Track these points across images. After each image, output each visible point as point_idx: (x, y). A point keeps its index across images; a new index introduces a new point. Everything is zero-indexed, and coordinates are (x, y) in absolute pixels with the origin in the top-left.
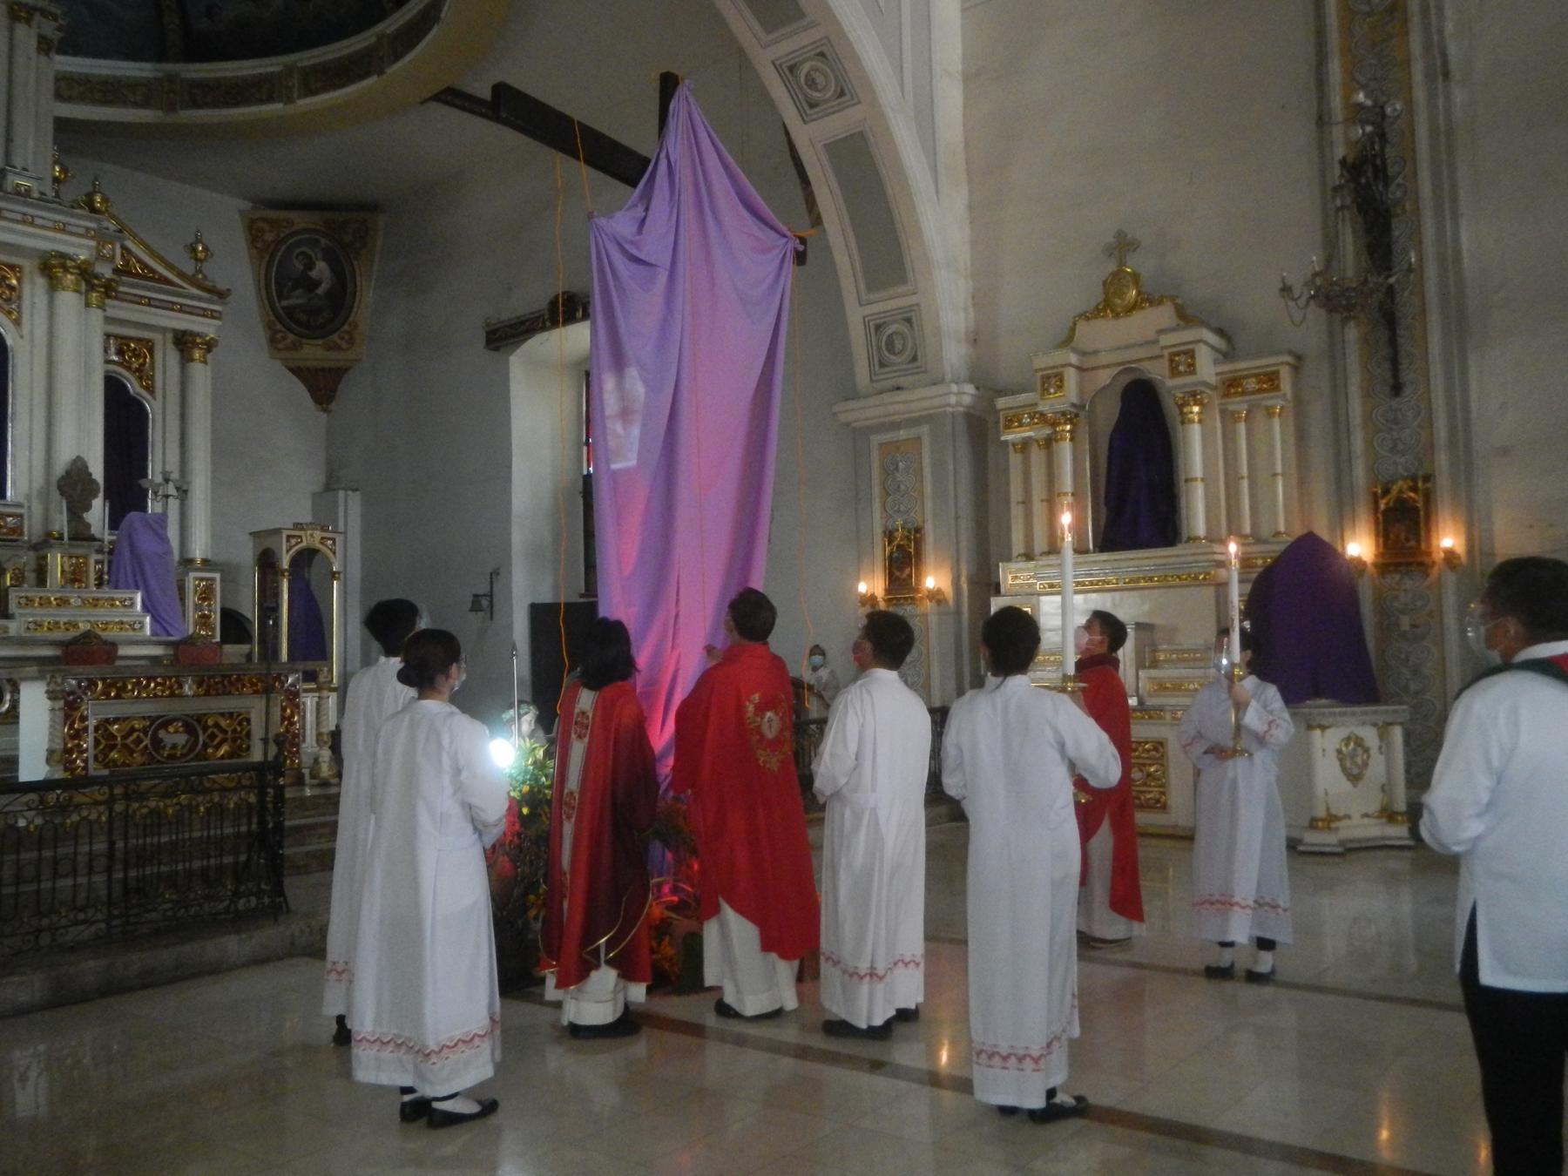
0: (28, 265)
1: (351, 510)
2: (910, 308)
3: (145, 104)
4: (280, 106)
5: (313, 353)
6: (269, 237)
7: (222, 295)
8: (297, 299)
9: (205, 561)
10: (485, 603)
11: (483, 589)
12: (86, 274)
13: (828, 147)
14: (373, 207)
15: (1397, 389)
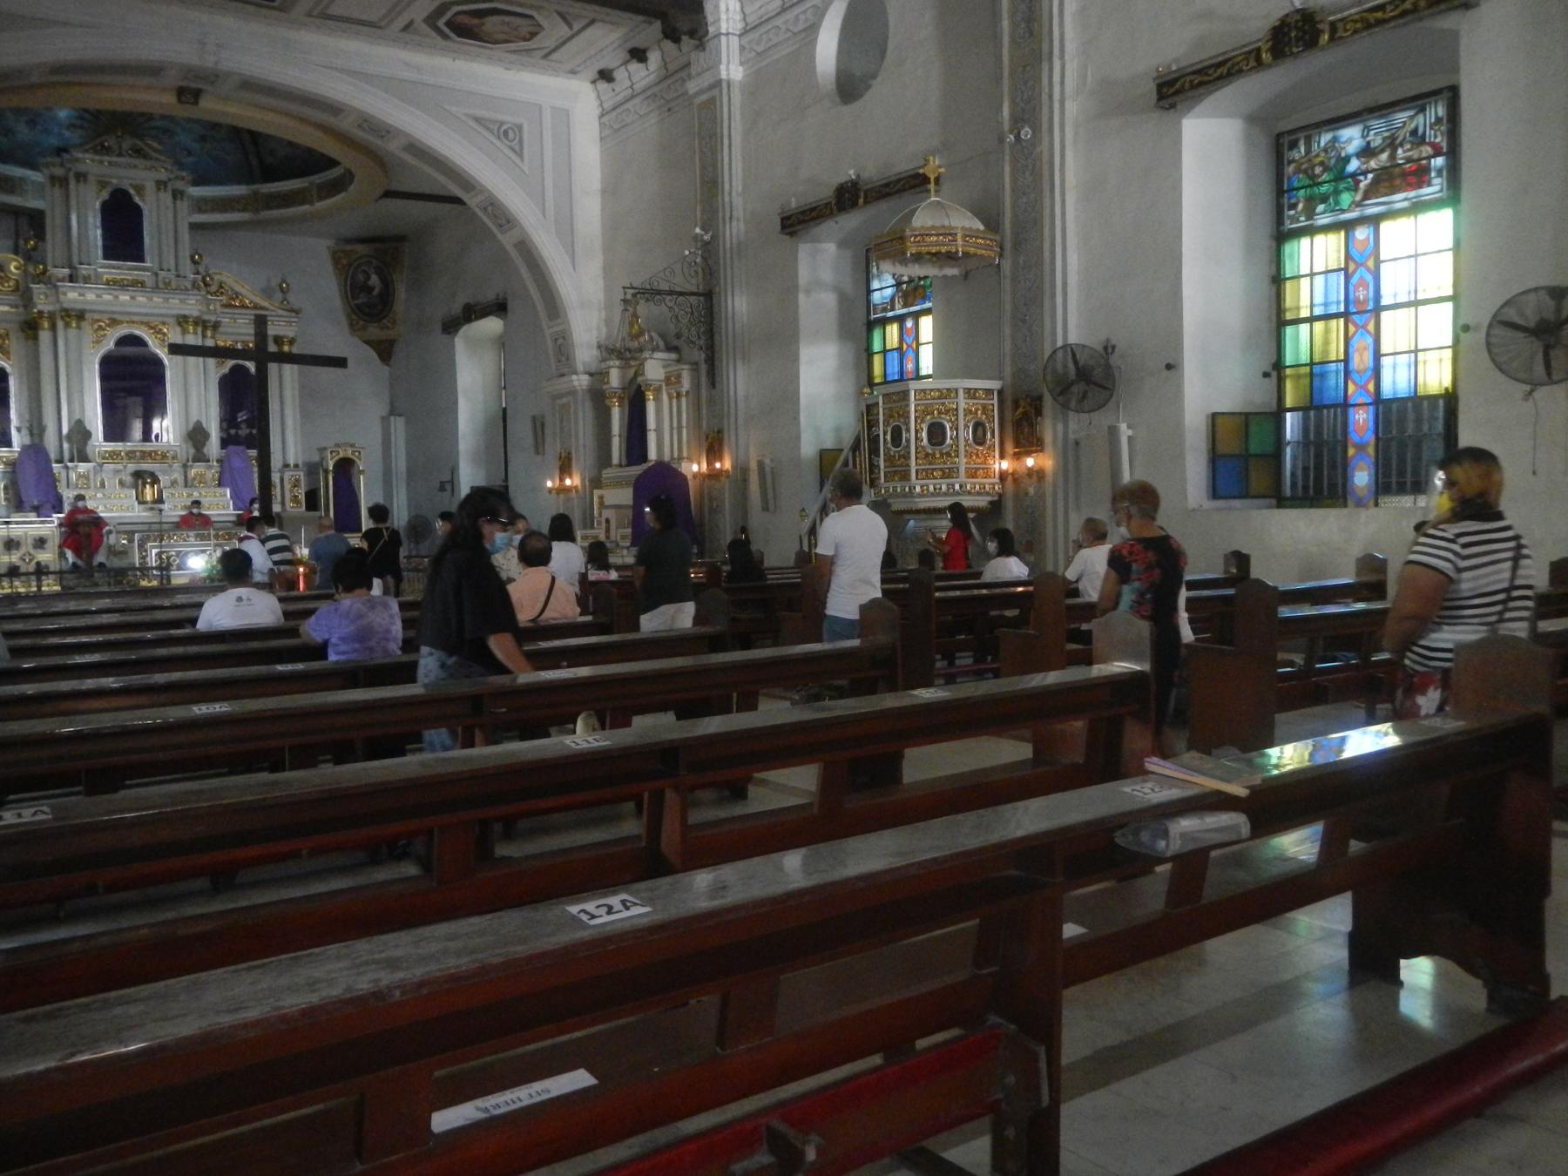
0: (172, 320)
1: (399, 425)
2: (564, 331)
3: (244, 210)
4: (306, 207)
5: (374, 331)
6: (345, 262)
7: (297, 312)
8: (362, 299)
9: (296, 466)
10: (448, 487)
11: (448, 478)
12: (196, 323)
13: (515, 246)
14: (401, 239)
15: (713, 384)
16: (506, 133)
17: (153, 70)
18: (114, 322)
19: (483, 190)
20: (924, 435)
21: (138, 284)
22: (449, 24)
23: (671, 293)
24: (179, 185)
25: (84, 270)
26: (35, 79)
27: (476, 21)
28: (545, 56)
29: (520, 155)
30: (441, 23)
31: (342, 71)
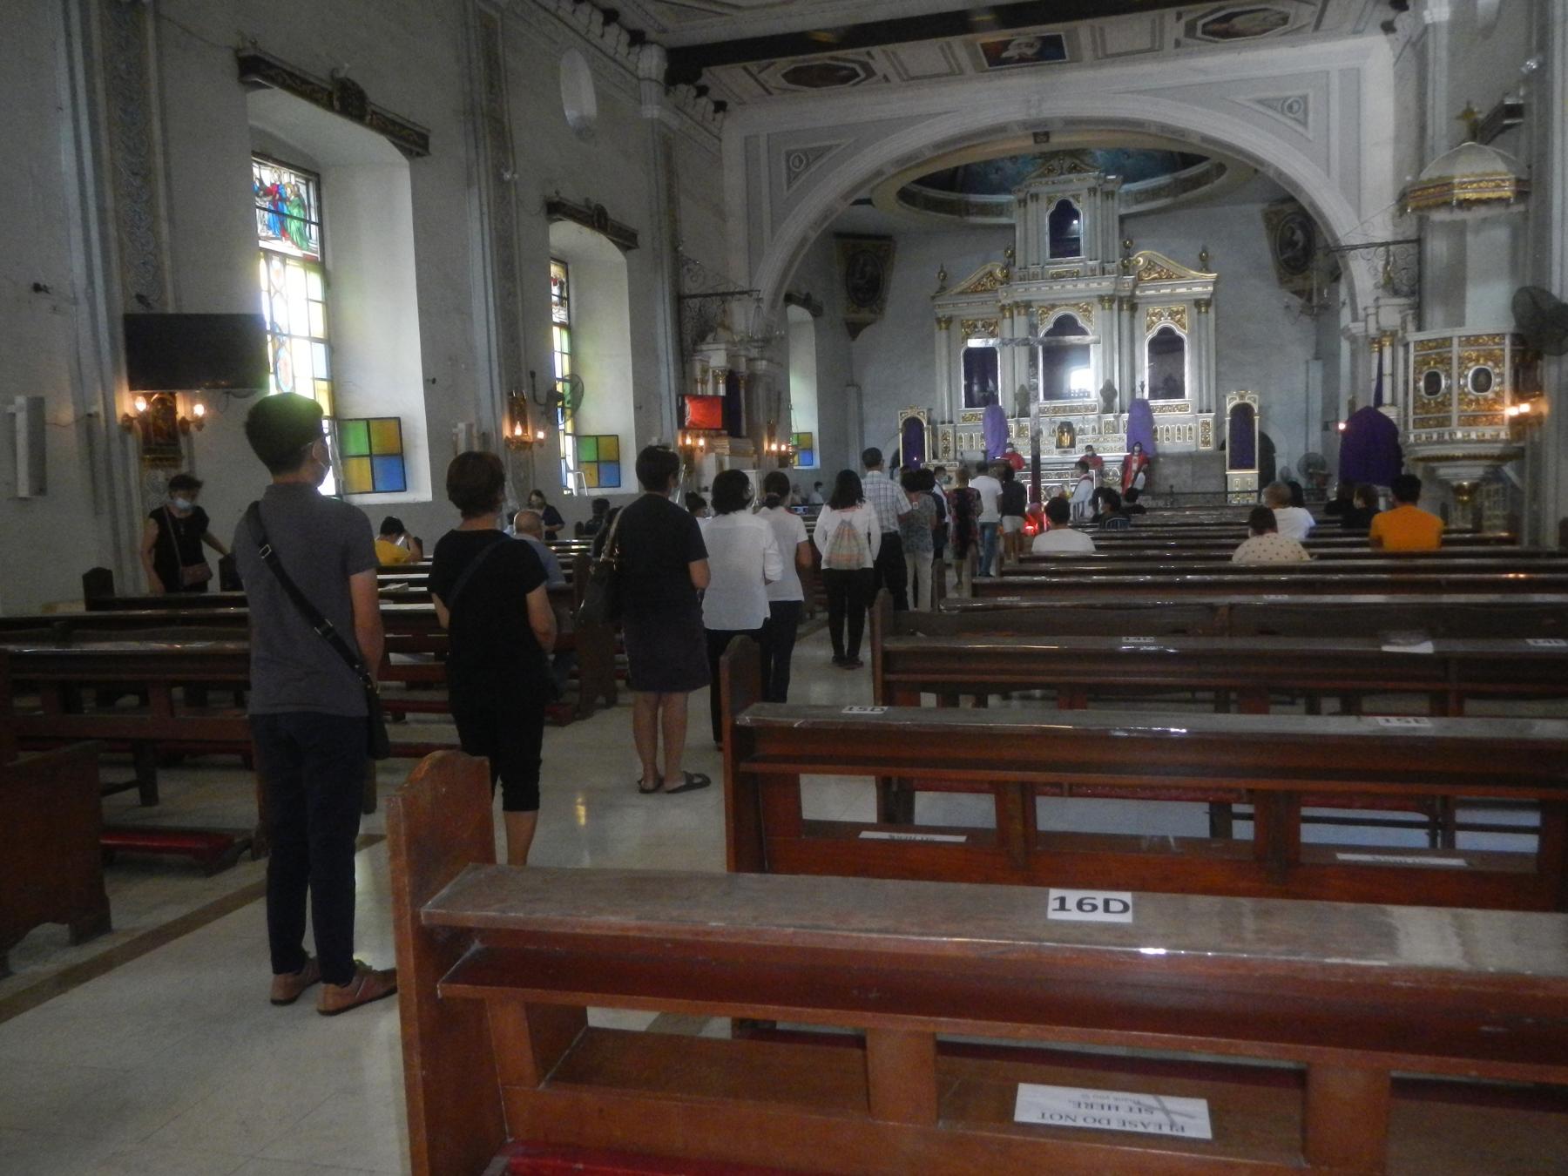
0: (1096, 300)
5: (1298, 282)
6: (1275, 221)
8: (1289, 254)
16: (1290, 107)
17: (1000, 130)
18: (1053, 307)
19: (1270, 165)
20: (1422, 384)
21: (1076, 275)
22: (1204, 32)
23: (1368, 246)
24: (1110, 187)
25: (1033, 269)
26: (928, 154)
27: (1225, 26)
28: (1317, 27)
29: (1305, 124)
30: (1199, 33)
31: (1145, 92)
